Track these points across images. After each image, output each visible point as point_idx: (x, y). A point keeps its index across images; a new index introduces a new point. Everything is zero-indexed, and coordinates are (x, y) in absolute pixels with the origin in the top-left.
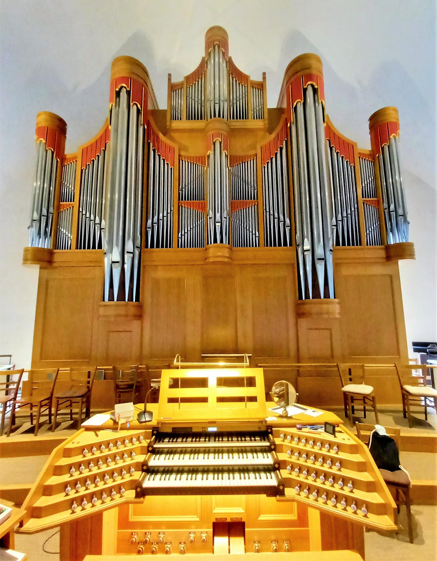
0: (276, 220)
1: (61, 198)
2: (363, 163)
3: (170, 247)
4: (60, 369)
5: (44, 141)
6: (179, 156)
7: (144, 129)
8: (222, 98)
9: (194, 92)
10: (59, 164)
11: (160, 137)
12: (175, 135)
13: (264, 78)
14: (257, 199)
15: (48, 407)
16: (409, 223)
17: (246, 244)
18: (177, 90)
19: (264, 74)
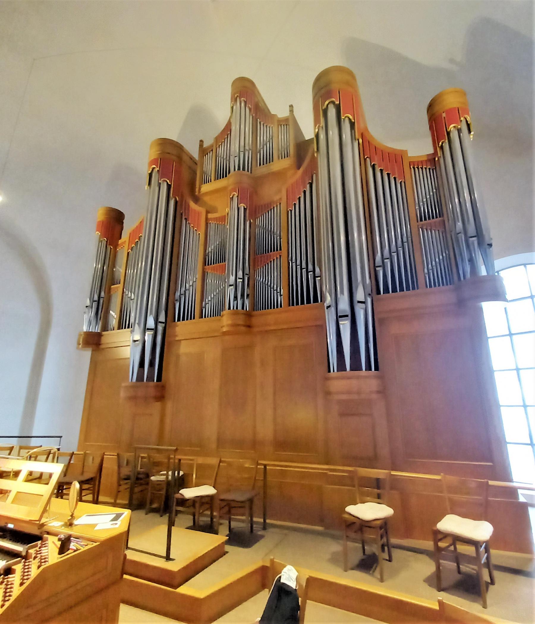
0: (304, 271)
1: (113, 281)
2: (420, 174)
3: (194, 318)
4: (105, 454)
5: (100, 234)
6: (207, 219)
7: (176, 203)
8: (247, 148)
9: (221, 151)
10: (112, 250)
11: (191, 206)
12: (206, 199)
13: (291, 111)
14: (280, 249)
15: (91, 492)
16: (490, 245)
17: (269, 305)
18: (209, 153)
19: (291, 106)
